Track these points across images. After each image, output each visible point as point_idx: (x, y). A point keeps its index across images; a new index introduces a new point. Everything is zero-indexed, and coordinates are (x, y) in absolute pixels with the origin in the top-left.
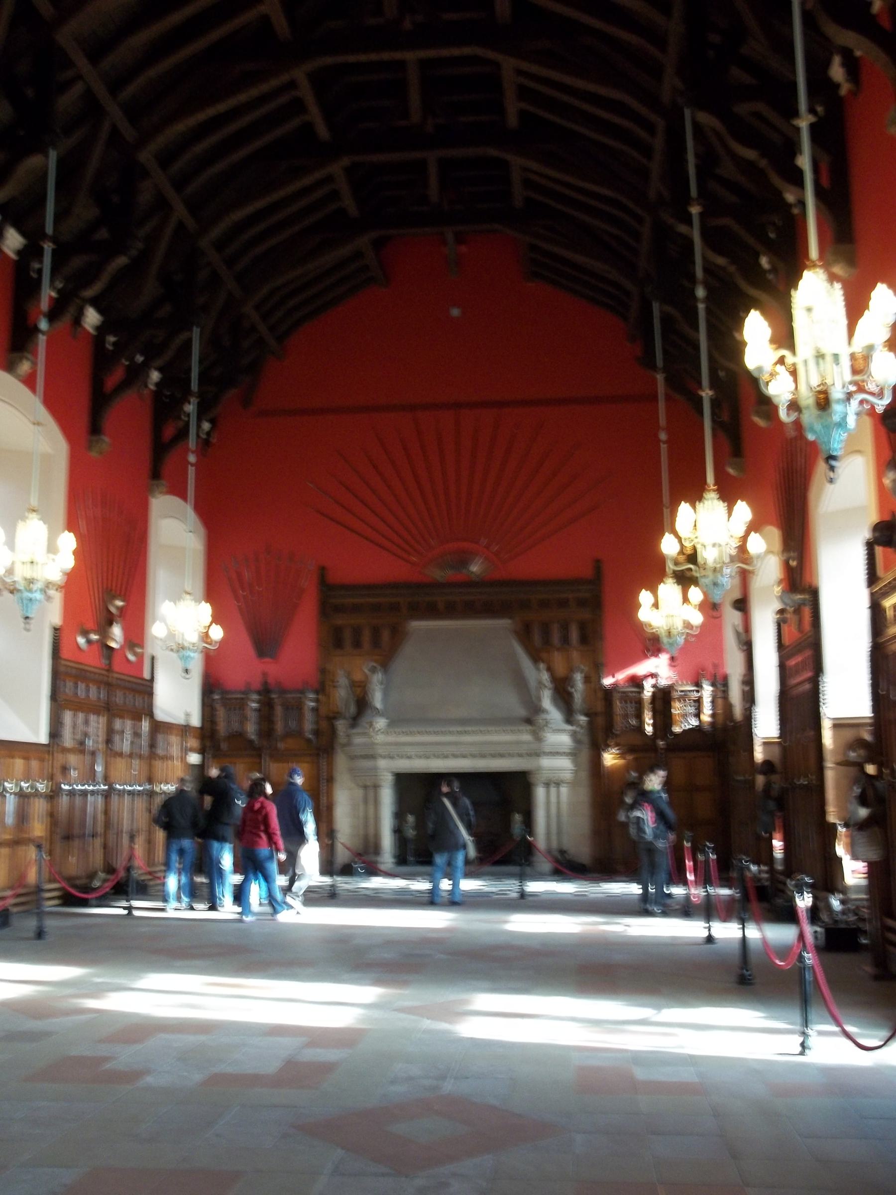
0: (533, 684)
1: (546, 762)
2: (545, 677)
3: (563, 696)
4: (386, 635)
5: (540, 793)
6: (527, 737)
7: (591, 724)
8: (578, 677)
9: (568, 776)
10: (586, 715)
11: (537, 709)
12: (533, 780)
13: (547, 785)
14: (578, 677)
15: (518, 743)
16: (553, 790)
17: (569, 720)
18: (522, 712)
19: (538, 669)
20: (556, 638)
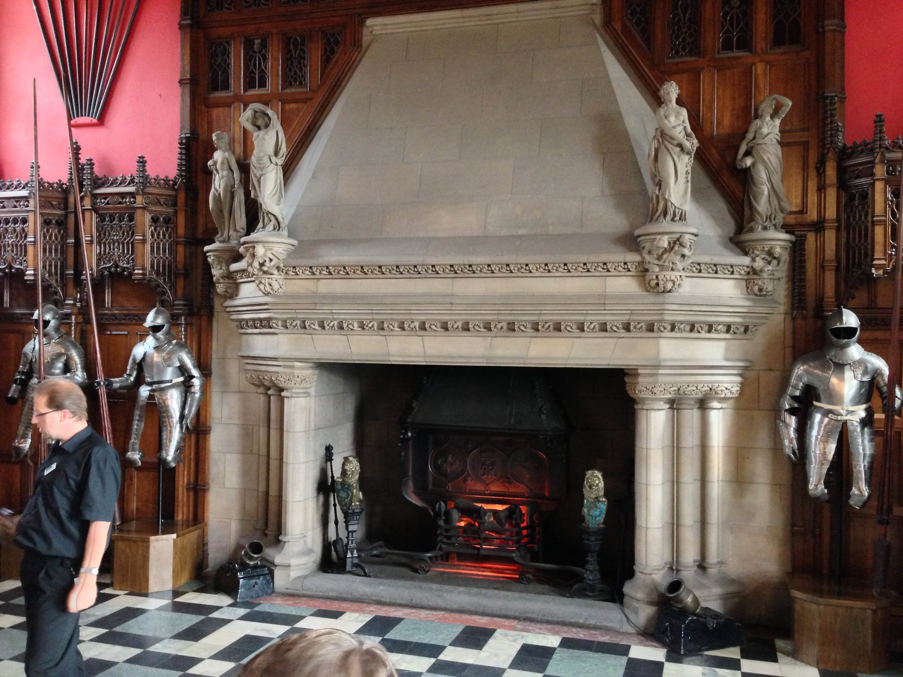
0: (644, 146)
1: (671, 349)
2: (678, 121)
3: (724, 173)
4: (315, 55)
5: (654, 425)
6: (624, 285)
7: (797, 250)
8: (769, 129)
9: (729, 383)
10: (787, 228)
11: (652, 208)
12: (641, 388)
13: (674, 404)
14: (769, 129)
15: (603, 300)
16: (691, 416)
17: (738, 241)
18: (615, 221)
19: (657, 100)
20: (712, 38)
